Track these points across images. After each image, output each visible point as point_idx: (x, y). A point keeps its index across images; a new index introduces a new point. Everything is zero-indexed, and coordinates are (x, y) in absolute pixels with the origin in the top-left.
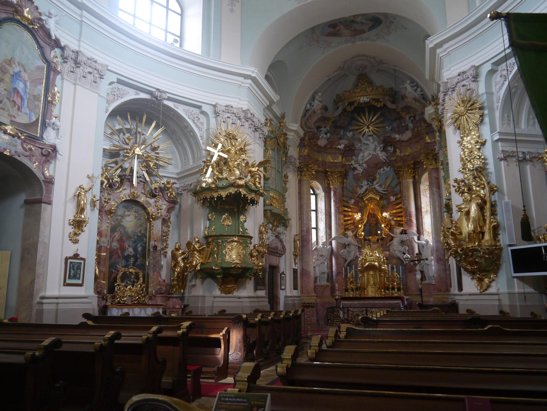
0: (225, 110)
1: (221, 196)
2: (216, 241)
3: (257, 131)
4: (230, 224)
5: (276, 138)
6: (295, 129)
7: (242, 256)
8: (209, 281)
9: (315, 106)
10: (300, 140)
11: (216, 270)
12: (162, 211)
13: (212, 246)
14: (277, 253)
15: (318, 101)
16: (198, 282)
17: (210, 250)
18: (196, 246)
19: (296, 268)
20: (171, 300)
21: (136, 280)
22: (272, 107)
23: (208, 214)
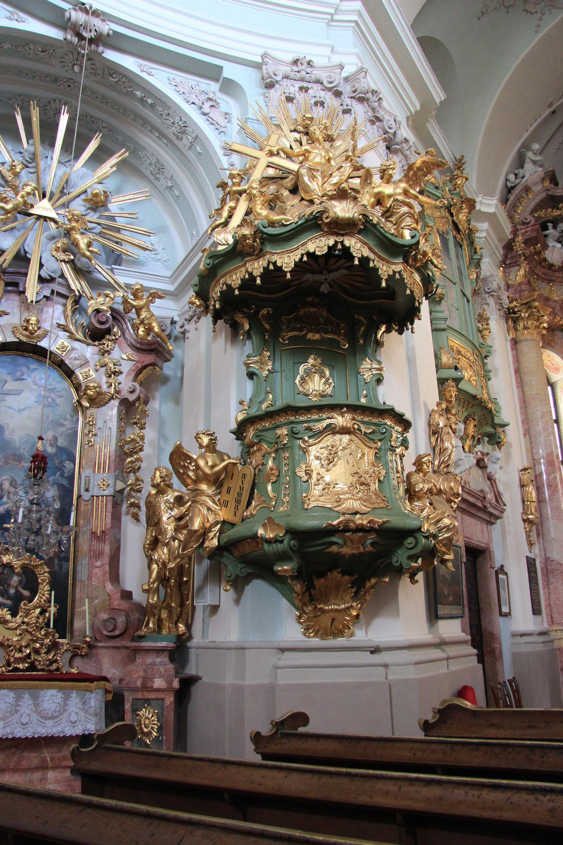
0: (292, 75)
1: (278, 269)
2: (269, 436)
3: (396, 152)
4: (329, 391)
5: (448, 208)
6: (492, 210)
7: (375, 486)
8: (258, 589)
9: (527, 176)
10: (504, 248)
11: (269, 541)
12: (121, 378)
13: (259, 455)
14: (484, 509)
15: (535, 163)
16: (226, 596)
17: (250, 471)
18: (201, 463)
19: (532, 556)
20: (139, 660)
21: (26, 593)
22: (428, 125)
23: (248, 357)
